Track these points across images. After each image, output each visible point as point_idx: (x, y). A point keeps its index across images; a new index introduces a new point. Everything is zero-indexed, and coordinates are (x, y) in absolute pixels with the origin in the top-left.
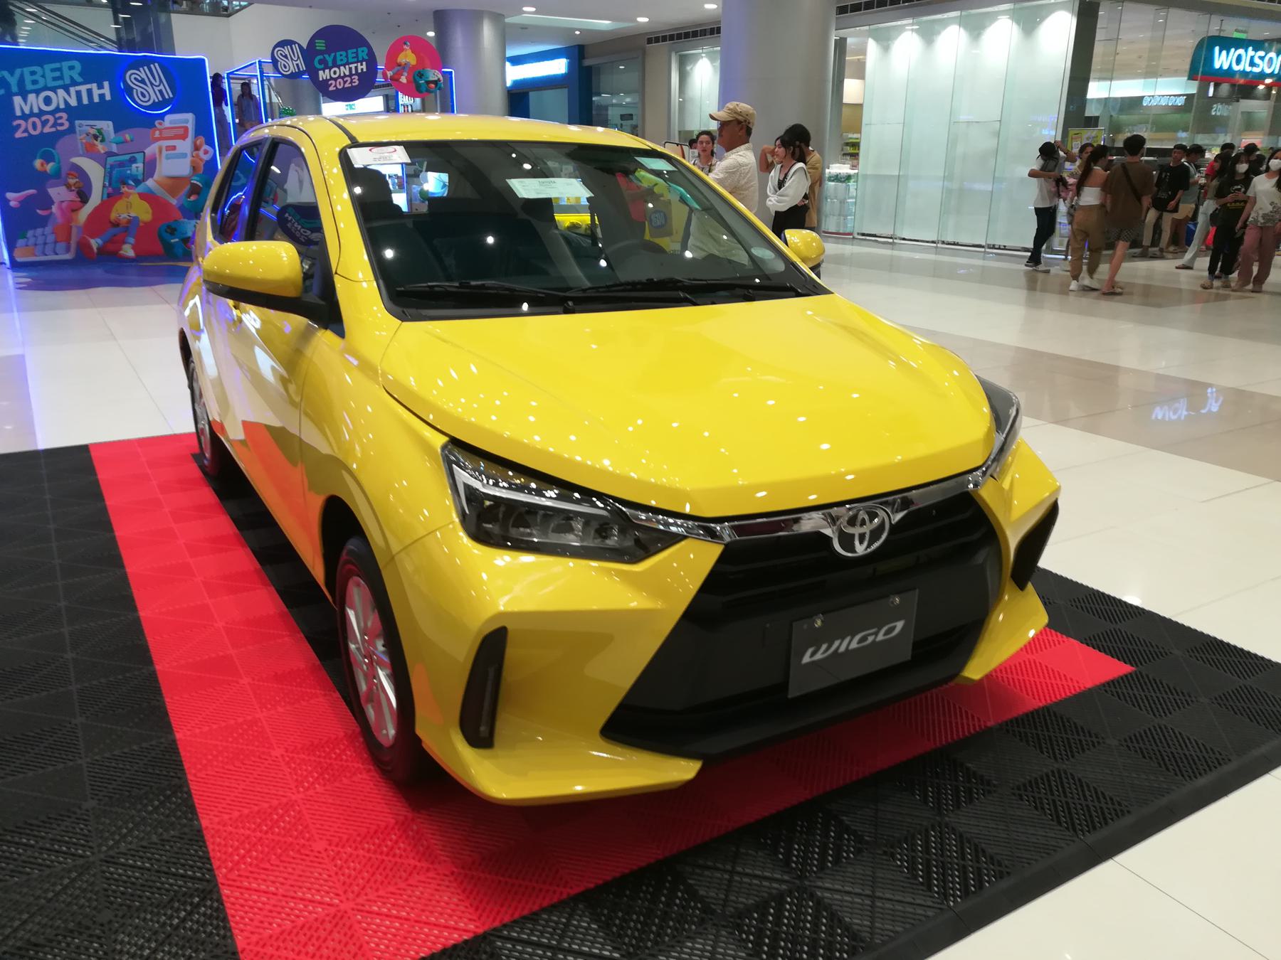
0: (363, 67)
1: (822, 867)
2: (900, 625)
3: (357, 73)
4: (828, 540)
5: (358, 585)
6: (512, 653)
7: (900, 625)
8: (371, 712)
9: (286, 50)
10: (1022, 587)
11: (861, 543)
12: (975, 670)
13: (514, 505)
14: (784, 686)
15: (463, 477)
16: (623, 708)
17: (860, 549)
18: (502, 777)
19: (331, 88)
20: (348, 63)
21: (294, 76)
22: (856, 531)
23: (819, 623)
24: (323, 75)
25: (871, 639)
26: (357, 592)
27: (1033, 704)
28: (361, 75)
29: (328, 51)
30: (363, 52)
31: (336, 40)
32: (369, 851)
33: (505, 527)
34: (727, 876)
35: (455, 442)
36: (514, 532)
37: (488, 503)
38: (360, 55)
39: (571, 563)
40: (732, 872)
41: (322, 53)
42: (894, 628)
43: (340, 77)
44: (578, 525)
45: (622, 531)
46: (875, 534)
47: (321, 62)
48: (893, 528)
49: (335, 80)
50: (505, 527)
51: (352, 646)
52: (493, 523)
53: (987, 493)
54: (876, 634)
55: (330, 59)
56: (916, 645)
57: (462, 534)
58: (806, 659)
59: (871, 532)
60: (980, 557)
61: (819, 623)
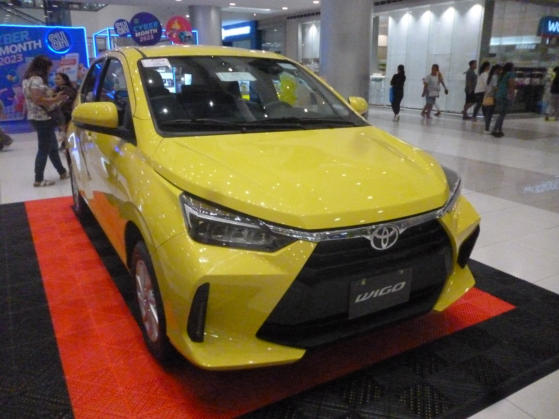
1: (364, 403)
2: (403, 284)
3: (153, 34)
4: (369, 241)
5: (141, 264)
6: (213, 296)
7: (403, 284)
8: (147, 325)
9: (121, 24)
10: (463, 267)
11: (385, 243)
12: (440, 306)
13: (214, 224)
14: (346, 314)
15: (189, 210)
16: (266, 324)
17: (384, 246)
18: (208, 356)
19: (141, 40)
20: (149, 29)
21: (125, 35)
22: (382, 237)
23: (363, 283)
24: (137, 35)
25: (389, 291)
26: (141, 268)
27: (469, 324)
28: (155, 35)
29: (140, 24)
30: (156, 24)
31: (144, 19)
32: (144, 392)
33: (210, 234)
34: (317, 406)
35: (186, 193)
36: (214, 237)
37: (201, 222)
38: (155, 25)
39: (242, 252)
40: (320, 405)
42: (401, 285)
43: (145, 35)
44: (245, 233)
45: (267, 237)
46: (392, 239)
47: (136, 29)
48: (401, 236)
49: (143, 36)
50: (210, 234)
51: (139, 294)
52: (203, 232)
53: (445, 220)
54: (392, 288)
55: (140, 27)
56: (412, 294)
57: (188, 237)
58: (358, 300)
59: (390, 238)
60: (442, 252)
61: (363, 283)
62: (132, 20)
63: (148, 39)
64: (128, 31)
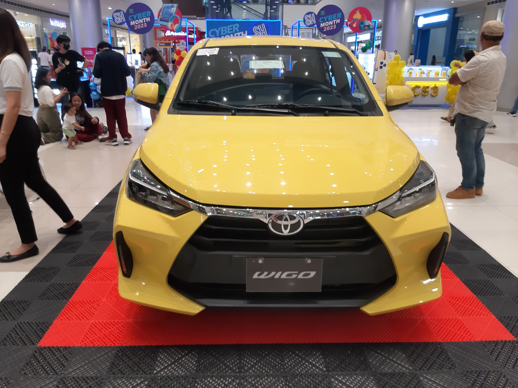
0: (148, 19)
3: (146, 22)
9: (118, 14)
19: (136, 28)
20: (142, 18)
28: (148, 23)
29: (134, 14)
38: (148, 14)
41: (132, 14)
43: (139, 24)
49: (137, 25)
55: (135, 17)
62: (128, 10)
63: (142, 27)
64: (124, 20)
